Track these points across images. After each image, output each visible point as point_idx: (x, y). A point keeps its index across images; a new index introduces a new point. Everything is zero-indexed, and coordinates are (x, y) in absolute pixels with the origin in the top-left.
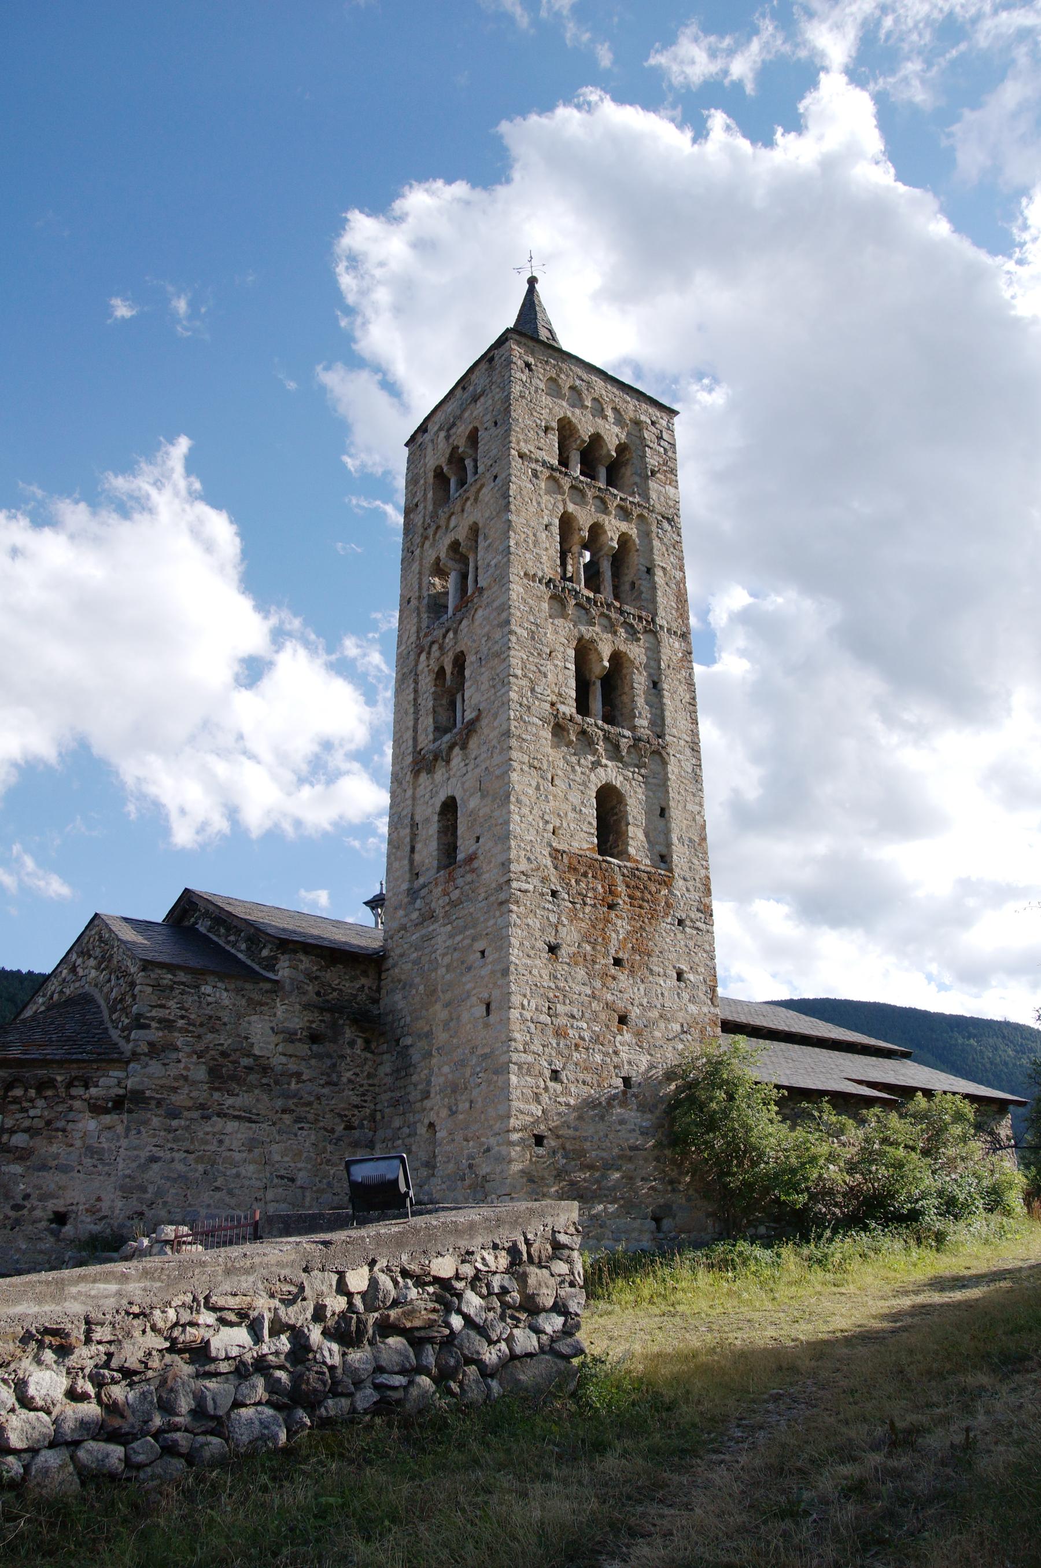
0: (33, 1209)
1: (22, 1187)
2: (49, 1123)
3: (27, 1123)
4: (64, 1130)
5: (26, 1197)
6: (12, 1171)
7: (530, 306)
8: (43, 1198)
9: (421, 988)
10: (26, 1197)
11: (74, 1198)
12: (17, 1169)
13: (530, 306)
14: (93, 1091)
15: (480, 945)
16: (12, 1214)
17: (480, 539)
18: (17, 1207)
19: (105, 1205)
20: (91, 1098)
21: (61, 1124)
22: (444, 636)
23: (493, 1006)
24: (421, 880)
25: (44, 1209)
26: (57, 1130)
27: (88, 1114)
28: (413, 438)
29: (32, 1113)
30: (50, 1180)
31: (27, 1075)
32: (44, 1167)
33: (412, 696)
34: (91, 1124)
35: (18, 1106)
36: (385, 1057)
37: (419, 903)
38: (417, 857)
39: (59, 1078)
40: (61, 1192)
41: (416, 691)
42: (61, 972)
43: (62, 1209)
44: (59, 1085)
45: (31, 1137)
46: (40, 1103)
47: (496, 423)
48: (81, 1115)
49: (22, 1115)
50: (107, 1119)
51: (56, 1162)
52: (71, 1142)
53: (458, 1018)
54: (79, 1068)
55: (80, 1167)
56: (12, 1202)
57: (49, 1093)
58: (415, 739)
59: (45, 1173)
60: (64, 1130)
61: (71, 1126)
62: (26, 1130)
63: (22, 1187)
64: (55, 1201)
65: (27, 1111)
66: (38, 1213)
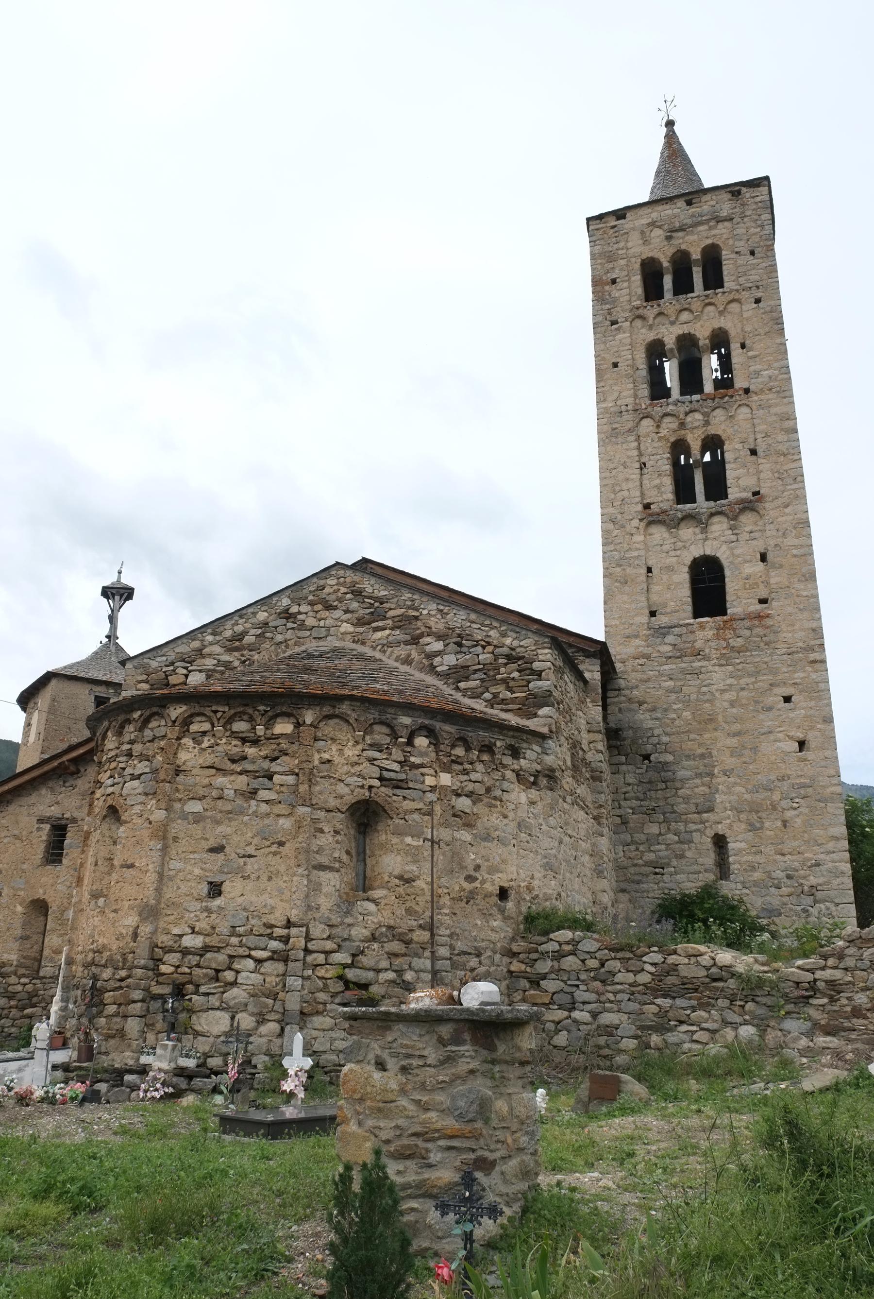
0: (483, 882)
1: (473, 857)
2: (488, 790)
3: (470, 787)
4: (501, 801)
5: (477, 868)
6: (463, 838)
7: (674, 153)
8: (492, 870)
9: (687, 714)
10: (477, 868)
11: (512, 873)
12: (465, 836)
13: (674, 153)
14: (523, 762)
15: (787, 691)
16: (466, 885)
17: (735, 347)
18: (470, 879)
19: (536, 883)
20: (521, 769)
21: (498, 793)
22: (687, 414)
23: (812, 743)
24: (662, 620)
25: (493, 883)
26: (495, 798)
27: (516, 787)
28: (601, 217)
29: (474, 776)
30: (496, 851)
31: (470, 734)
32: (487, 838)
33: (636, 453)
34: (519, 796)
35: (460, 767)
36: (624, 768)
37: (670, 639)
38: (654, 598)
39: (499, 744)
40: (503, 866)
41: (639, 448)
42: (254, 614)
43: (506, 885)
44: (496, 750)
45: (474, 803)
46: (480, 767)
47: (752, 253)
48: (512, 786)
49: (466, 777)
50: (533, 793)
51: (497, 833)
52: (506, 812)
53: (755, 749)
54: (513, 737)
55: (514, 841)
56: (466, 873)
57: (485, 757)
58: (642, 494)
59: (489, 844)
60: (501, 801)
61: (505, 796)
62: (469, 795)
63: (473, 857)
64: (500, 875)
65: (468, 774)
66: (488, 887)
